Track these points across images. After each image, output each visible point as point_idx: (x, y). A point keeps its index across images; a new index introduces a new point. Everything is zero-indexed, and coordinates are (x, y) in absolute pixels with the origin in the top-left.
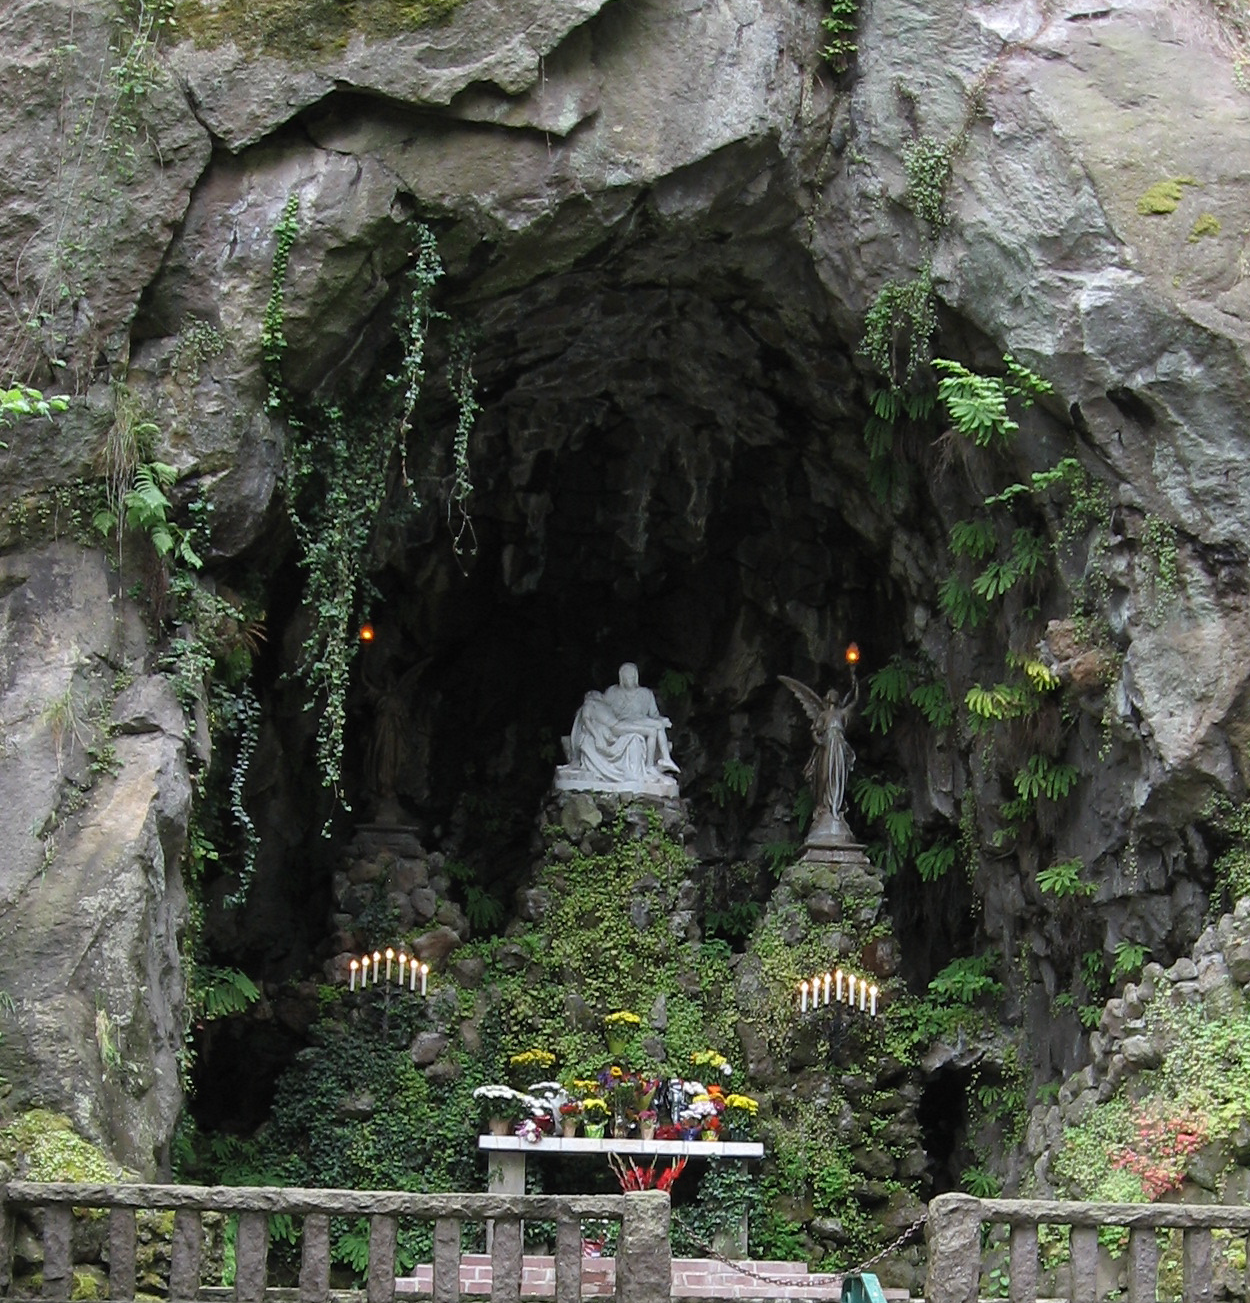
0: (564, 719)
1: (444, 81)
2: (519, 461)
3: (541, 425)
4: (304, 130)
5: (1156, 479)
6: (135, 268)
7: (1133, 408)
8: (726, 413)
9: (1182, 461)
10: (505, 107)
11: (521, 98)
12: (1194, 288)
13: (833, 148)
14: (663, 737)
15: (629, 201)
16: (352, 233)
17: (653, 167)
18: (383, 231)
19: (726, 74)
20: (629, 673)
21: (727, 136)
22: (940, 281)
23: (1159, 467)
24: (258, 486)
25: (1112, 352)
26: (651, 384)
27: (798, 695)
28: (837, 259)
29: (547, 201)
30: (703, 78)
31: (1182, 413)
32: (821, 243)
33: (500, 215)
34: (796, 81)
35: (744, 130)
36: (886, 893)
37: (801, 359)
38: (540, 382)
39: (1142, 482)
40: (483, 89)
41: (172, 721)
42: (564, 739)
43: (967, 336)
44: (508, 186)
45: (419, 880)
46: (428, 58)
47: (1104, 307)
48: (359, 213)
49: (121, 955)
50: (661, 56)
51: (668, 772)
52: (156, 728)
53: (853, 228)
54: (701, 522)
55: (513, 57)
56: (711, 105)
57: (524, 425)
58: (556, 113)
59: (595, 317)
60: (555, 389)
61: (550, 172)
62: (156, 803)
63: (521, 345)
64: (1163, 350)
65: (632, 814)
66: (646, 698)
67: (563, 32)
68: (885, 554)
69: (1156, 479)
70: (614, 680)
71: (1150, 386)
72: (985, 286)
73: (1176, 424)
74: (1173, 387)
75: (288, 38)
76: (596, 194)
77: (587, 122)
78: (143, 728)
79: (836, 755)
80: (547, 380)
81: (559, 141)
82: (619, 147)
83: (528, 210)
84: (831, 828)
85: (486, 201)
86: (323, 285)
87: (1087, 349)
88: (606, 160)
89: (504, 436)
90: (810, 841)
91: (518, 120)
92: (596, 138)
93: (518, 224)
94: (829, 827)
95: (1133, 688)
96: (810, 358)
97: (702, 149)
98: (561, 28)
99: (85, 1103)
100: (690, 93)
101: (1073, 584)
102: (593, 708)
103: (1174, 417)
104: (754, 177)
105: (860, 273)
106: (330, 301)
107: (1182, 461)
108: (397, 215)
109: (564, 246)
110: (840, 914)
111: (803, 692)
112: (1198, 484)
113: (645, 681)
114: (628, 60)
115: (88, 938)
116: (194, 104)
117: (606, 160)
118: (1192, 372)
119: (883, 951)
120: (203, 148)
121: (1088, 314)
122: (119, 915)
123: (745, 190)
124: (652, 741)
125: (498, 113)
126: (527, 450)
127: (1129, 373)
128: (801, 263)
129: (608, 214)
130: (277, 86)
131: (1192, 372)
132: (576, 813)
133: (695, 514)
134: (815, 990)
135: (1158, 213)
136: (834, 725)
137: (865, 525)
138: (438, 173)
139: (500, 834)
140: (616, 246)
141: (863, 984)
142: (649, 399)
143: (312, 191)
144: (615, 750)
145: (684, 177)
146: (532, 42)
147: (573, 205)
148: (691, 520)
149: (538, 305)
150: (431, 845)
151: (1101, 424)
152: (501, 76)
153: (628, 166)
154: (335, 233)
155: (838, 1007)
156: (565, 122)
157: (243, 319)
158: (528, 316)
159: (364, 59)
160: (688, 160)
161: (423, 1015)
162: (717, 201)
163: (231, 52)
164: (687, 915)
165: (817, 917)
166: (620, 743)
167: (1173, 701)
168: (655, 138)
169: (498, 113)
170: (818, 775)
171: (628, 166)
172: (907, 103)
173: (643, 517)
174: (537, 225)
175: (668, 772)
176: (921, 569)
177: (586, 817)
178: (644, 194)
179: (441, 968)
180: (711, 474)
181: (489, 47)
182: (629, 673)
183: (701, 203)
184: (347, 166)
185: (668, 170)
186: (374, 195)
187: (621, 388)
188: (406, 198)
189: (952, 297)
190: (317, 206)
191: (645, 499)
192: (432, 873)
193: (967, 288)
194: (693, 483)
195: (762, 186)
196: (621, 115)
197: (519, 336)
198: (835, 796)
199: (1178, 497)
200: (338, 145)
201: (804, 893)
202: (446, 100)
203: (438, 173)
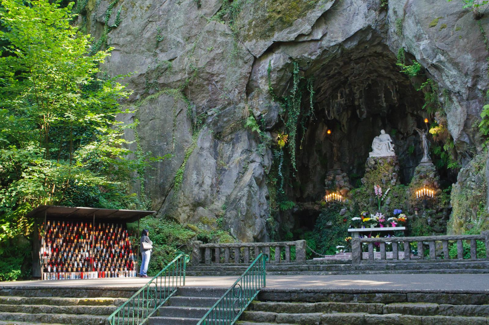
2: (356, 93)
3: (358, 86)
4: (270, 50)
5: (444, 81)
6: (244, 82)
9: (447, 76)
10: (307, 37)
11: (310, 34)
12: (440, 41)
13: (384, 25)
14: (390, 144)
15: (337, 47)
16: (281, 67)
17: (340, 40)
18: (287, 65)
19: (356, 17)
20: (383, 131)
21: (358, 29)
22: (404, 47)
23: (444, 78)
24: (274, 115)
29: (319, 52)
30: (351, 19)
31: (444, 66)
33: (309, 57)
34: (374, 14)
35: (361, 27)
39: (442, 82)
43: (409, 57)
44: (310, 51)
45: (341, 179)
46: (289, 33)
48: (281, 64)
49: (244, 203)
50: (341, 18)
52: (255, 161)
54: (395, 98)
55: (306, 28)
56: (353, 24)
57: (355, 86)
58: (317, 36)
61: (318, 46)
64: (436, 55)
65: (380, 161)
66: (388, 136)
67: (315, 21)
69: (444, 81)
70: (380, 134)
71: (437, 62)
72: (410, 47)
74: (440, 61)
75: (264, 36)
76: (329, 48)
77: (324, 35)
78: (253, 161)
81: (317, 41)
82: (332, 38)
83: (315, 55)
85: (306, 55)
86: (277, 77)
87: (424, 57)
88: (330, 41)
91: (309, 39)
92: (327, 38)
93: (314, 57)
98: (314, 20)
99: (232, 229)
102: (376, 140)
103: (443, 67)
104: (368, 34)
105: (395, 48)
106: (280, 80)
107: (447, 76)
108: (289, 62)
109: (324, 59)
110: (425, 177)
112: (451, 80)
113: (386, 133)
114: (333, 21)
115: (238, 200)
116: (250, 52)
117: (330, 41)
118: (442, 58)
119: (436, 183)
120: (253, 59)
122: (244, 196)
123: (366, 38)
125: (305, 39)
127: (432, 60)
128: (385, 47)
129: (333, 51)
130: (263, 45)
131: (442, 58)
133: (394, 97)
134: (419, 193)
135: (433, 26)
138: (295, 52)
139: (358, 169)
141: (427, 190)
142: (377, 77)
143: (276, 60)
144: (380, 148)
146: (309, 24)
147: (325, 51)
150: (342, 171)
151: (432, 71)
152: (304, 32)
153: (335, 41)
154: (278, 68)
155: (426, 196)
156: (319, 37)
157: (264, 86)
159: (278, 36)
160: (349, 36)
161: (342, 206)
162: (359, 42)
163: (254, 41)
164: (395, 180)
165: (421, 178)
166: (381, 146)
167: (454, 126)
168: (340, 34)
169: (305, 39)
170: (422, 147)
171: (335, 41)
172: (395, 12)
173: (384, 99)
174: (317, 57)
179: (346, 195)
180: (394, 89)
181: (301, 27)
182: (383, 131)
183: (355, 43)
184: (278, 55)
185: (344, 39)
186: (284, 59)
188: (291, 58)
189: (406, 49)
190: (274, 64)
191: (383, 96)
192: (343, 177)
193: (408, 48)
195: (370, 36)
196: (332, 32)
199: (448, 84)
200: (277, 52)
201: (419, 172)
202: (294, 39)
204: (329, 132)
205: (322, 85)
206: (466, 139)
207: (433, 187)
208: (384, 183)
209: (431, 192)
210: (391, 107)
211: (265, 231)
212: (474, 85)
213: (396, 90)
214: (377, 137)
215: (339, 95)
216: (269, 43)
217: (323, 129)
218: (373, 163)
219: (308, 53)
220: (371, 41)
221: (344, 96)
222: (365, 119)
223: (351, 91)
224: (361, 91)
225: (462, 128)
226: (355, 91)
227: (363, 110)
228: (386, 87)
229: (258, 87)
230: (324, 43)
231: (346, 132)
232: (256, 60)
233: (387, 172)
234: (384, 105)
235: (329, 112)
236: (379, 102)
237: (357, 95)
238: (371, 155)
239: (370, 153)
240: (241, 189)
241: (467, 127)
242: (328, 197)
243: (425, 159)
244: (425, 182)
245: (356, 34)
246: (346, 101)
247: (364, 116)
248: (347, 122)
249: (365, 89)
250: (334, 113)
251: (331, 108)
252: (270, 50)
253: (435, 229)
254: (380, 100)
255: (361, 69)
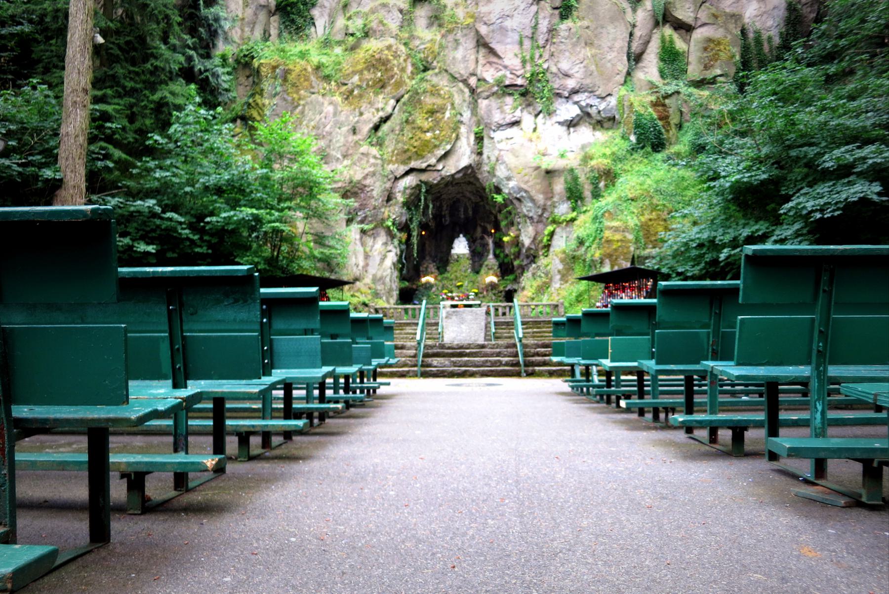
0: (452, 242)
1: (424, 166)
4: (407, 173)
6: (386, 193)
7: (519, 200)
8: (472, 198)
11: (434, 166)
13: (479, 164)
17: (453, 172)
18: (418, 185)
20: (461, 235)
24: (404, 219)
29: (439, 179)
32: (479, 176)
34: (474, 156)
40: (429, 166)
41: (394, 250)
43: (498, 190)
45: (432, 267)
48: (414, 183)
53: (483, 176)
55: (433, 161)
72: (500, 183)
74: (522, 196)
75: (404, 162)
78: (390, 251)
79: (491, 245)
84: (491, 256)
92: (445, 169)
93: (435, 182)
97: (460, 168)
98: (439, 156)
100: (458, 161)
101: (515, 223)
106: (411, 195)
110: (491, 269)
128: (478, 179)
130: (403, 169)
138: (424, 177)
139: (443, 261)
140: (451, 182)
143: (410, 181)
145: (458, 172)
147: (443, 179)
151: (515, 202)
157: (400, 198)
159: (414, 164)
163: (396, 165)
172: (489, 158)
178: (453, 175)
179: (436, 278)
182: (461, 235)
198: (491, 252)
203: (424, 177)
206: (533, 247)
207: (497, 276)
209: (495, 279)
210: (467, 218)
212: (542, 214)
216: (407, 168)
219: (432, 178)
220: (470, 174)
223: (441, 204)
230: (443, 173)
232: (396, 179)
233: (467, 264)
234: (462, 216)
237: (445, 208)
238: (453, 252)
240: (384, 271)
242: (424, 280)
244: (491, 272)
245: (463, 169)
252: (407, 173)
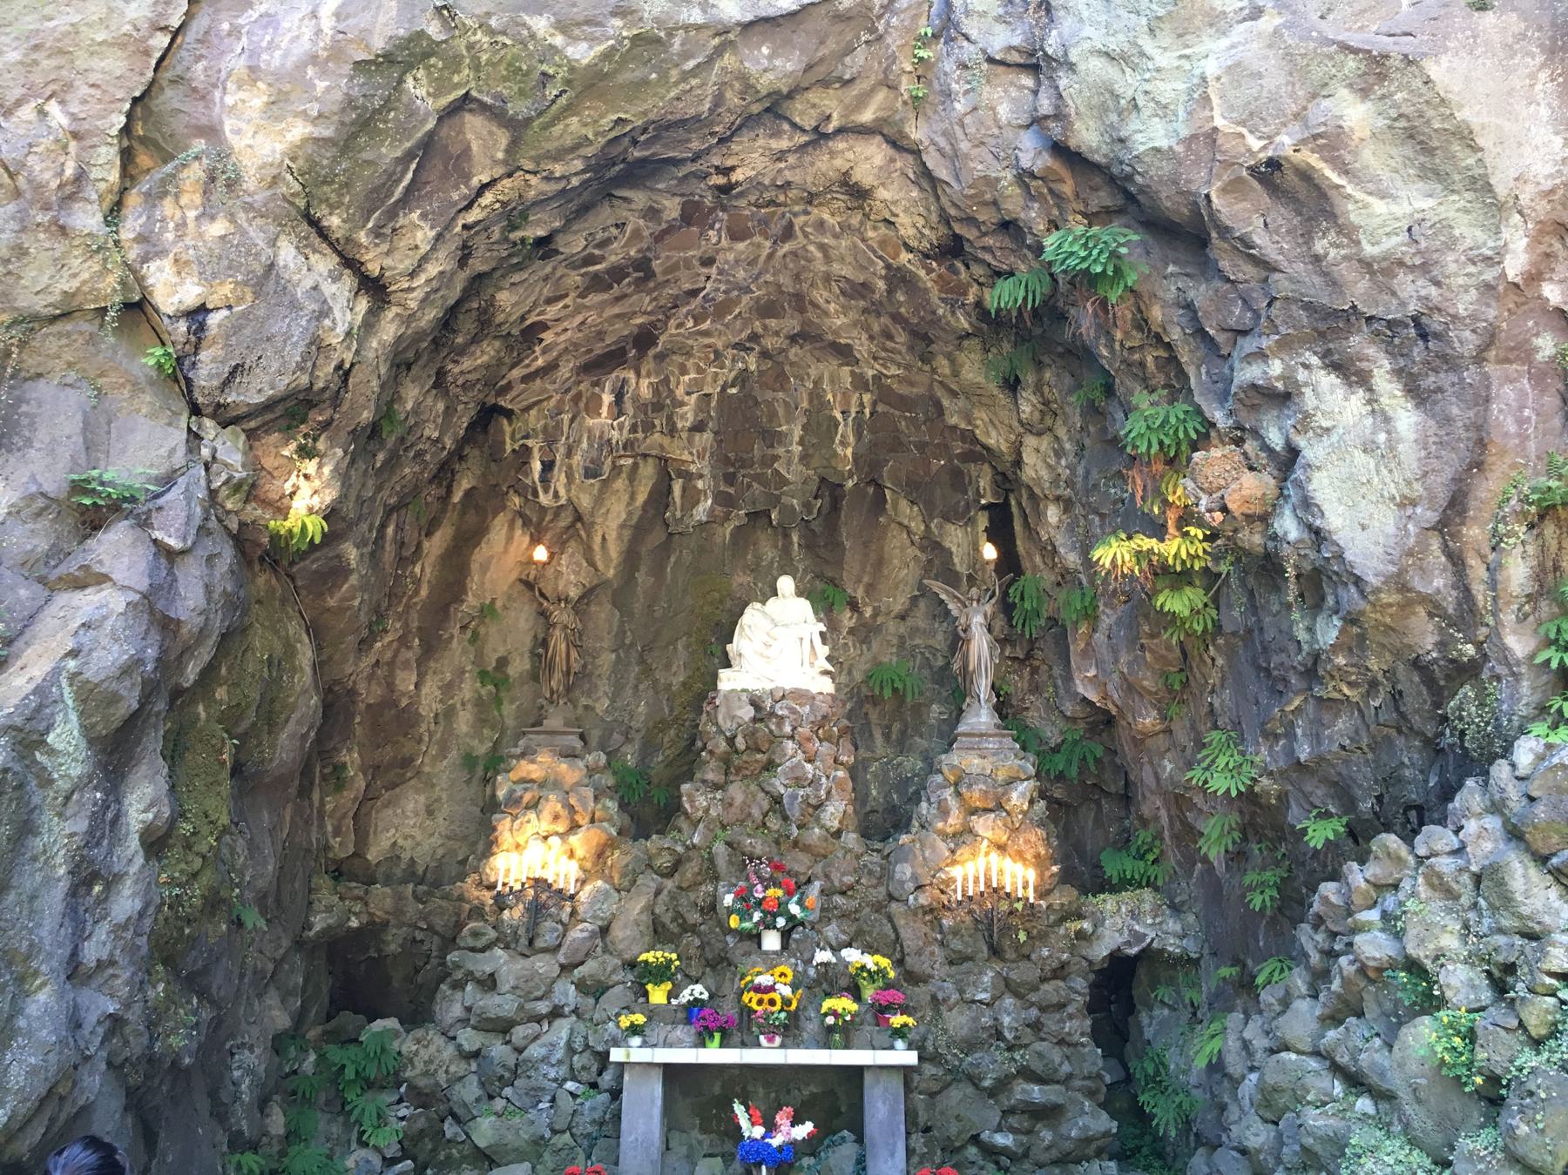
2: (682, 404)
3: (699, 370)
8: (862, 346)
14: (817, 640)
16: (379, 44)
20: (786, 584)
25: (1250, 118)
26: (792, 324)
27: (943, 597)
28: (942, 142)
31: (1345, 171)
33: (559, 40)
36: (1038, 776)
37: (922, 273)
38: (690, 324)
42: (729, 647)
47: (1238, 64)
51: (826, 673)
54: (849, 451)
57: (684, 371)
59: (724, 243)
60: (706, 334)
62: (72, 664)
63: (660, 278)
68: (1018, 463)
70: (775, 593)
73: (1338, 187)
80: (696, 324)
84: (981, 717)
85: (540, 24)
87: (1219, 122)
89: (666, 381)
90: (961, 729)
93: (582, 53)
94: (978, 715)
95: (1307, 503)
96: (929, 271)
102: (752, 616)
103: (1335, 178)
111: (947, 592)
121: (1218, 79)
124: (807, 643)
126: (688, 394)
132: (729, 709)
133: (844, 444)
136: (977, 620)
137: (996, 439)
142: (793, 339)
148: (839, 450)
149: (664, 226)
154: (363, 40)
158: (659, 238)
160: (771, 12)
173: (797, 449)
175: (826, 673)
176: (1049, 466)
177: (739, 713)
182: (786, 584)
185: (749, 17)
187: (765, 327)
191: (797, 433)
194: (839, 416)
197: (656, 264)
198: (983, 686)
204: (541, 553)
205: (552, 311)
208: (795, 813)
209: (1018, 876)
210: (830, 489)
211: (94, 1082)
213: (860, 412)
214: (758, 605)
215: (607, 398)
217: (510, 539)
218: (747, 713)
221: (629, 408)
222: (701, 524)
223: (663, 388)
224: (708, 395)
225: (1427, 515)
226: (680, 392)
227: (700, 484)
228: (816, 395)
229: (212, 132)
231: (611, 573)
235: (548, 466)
236: (776, 458)
237: (687, 415)
238: (728, 681)
239: (724, 674)
241: (1462, 512)
243: (981, 717)
246: (633, 429)
247: (701, 511)
248: (622, 526)
249: (724, 389)
250: (570, 476)
251: (562, 450)
253: (1037, 1066)
254: (781, 451)
255: (741, 274)
